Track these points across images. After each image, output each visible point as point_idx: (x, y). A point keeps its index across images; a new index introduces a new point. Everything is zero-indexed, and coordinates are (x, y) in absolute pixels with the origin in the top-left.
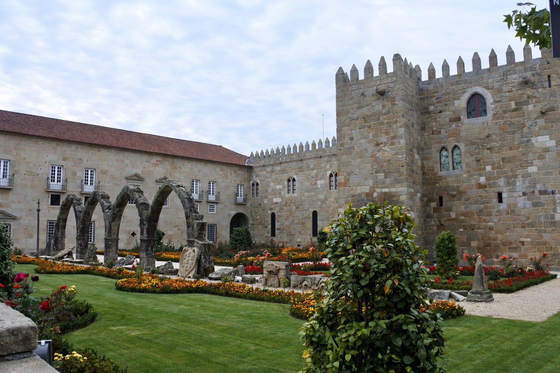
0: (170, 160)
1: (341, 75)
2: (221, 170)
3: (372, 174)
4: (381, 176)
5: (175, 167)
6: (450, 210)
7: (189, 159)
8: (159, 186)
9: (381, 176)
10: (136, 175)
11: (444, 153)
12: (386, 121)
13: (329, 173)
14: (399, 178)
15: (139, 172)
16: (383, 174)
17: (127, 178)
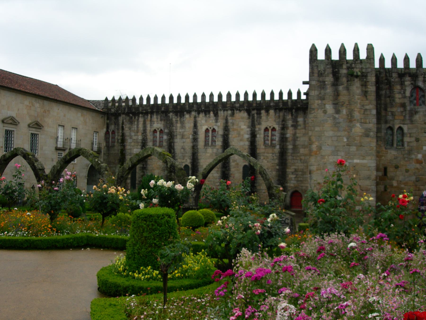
0: (41, 101)
1: (313, 51)
2: (82, 116)
3: (344, 146)
4: (353, 149)
5: (45, 110)
6: (392, 179)
7: (57, 102)
8: (31, 132)
9: (353, 149)
10: (12, 119)
11: (390, 132)
12: (359, 101)
13: (204, 128)
14: (370, 152)
15: (13, 114)
16: (355, 147)
17: (3, 121)
